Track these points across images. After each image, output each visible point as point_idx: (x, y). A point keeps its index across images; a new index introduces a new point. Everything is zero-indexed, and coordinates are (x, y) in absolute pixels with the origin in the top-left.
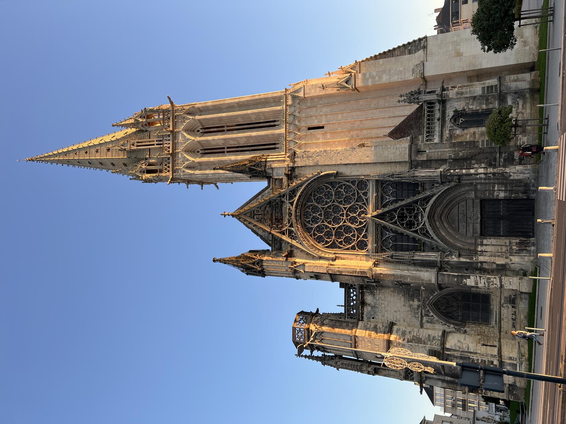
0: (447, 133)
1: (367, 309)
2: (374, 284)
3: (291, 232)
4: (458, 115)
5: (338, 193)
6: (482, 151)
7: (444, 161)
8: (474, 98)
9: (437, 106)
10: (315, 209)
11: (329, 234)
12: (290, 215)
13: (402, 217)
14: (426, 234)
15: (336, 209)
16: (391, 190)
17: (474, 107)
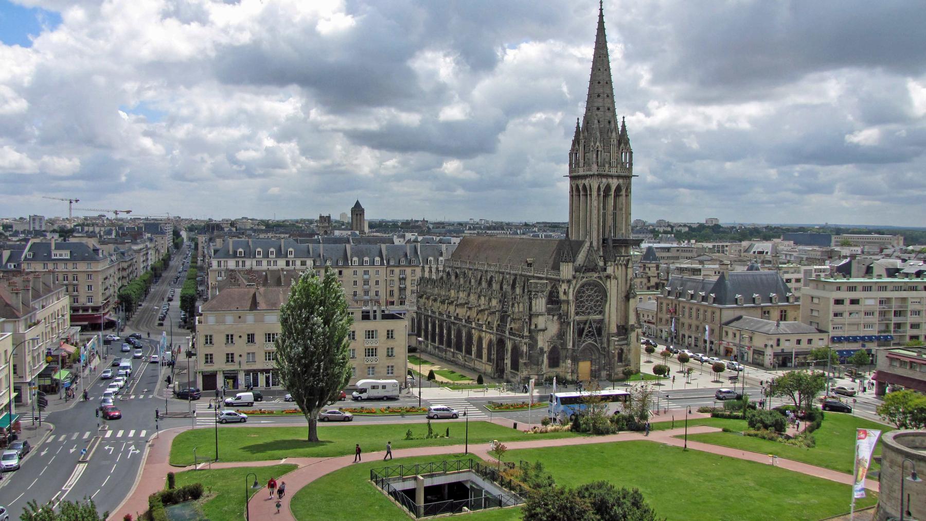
0: (617, 347)
1: (551, 317)
2: (563, 320)
3: (583, 277)
4: (622, 350)
5: (597, 301)
6: (610, 361)
7: (609, 346)
8: (626, 356)
9: (625, 342)
10: (592, 289)
11: (581, 297)
12: (591, 277)
13: (590, 332)
14: (584, 342)
15: (592, 300)
16: (598, 326)
17: (624, 356)
